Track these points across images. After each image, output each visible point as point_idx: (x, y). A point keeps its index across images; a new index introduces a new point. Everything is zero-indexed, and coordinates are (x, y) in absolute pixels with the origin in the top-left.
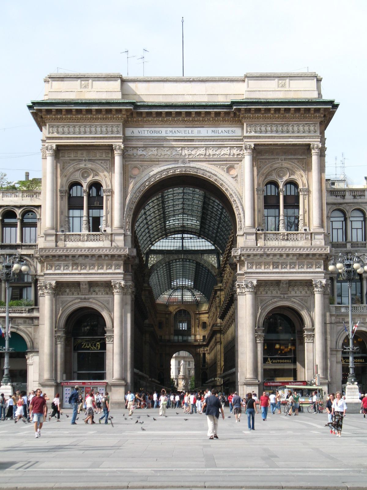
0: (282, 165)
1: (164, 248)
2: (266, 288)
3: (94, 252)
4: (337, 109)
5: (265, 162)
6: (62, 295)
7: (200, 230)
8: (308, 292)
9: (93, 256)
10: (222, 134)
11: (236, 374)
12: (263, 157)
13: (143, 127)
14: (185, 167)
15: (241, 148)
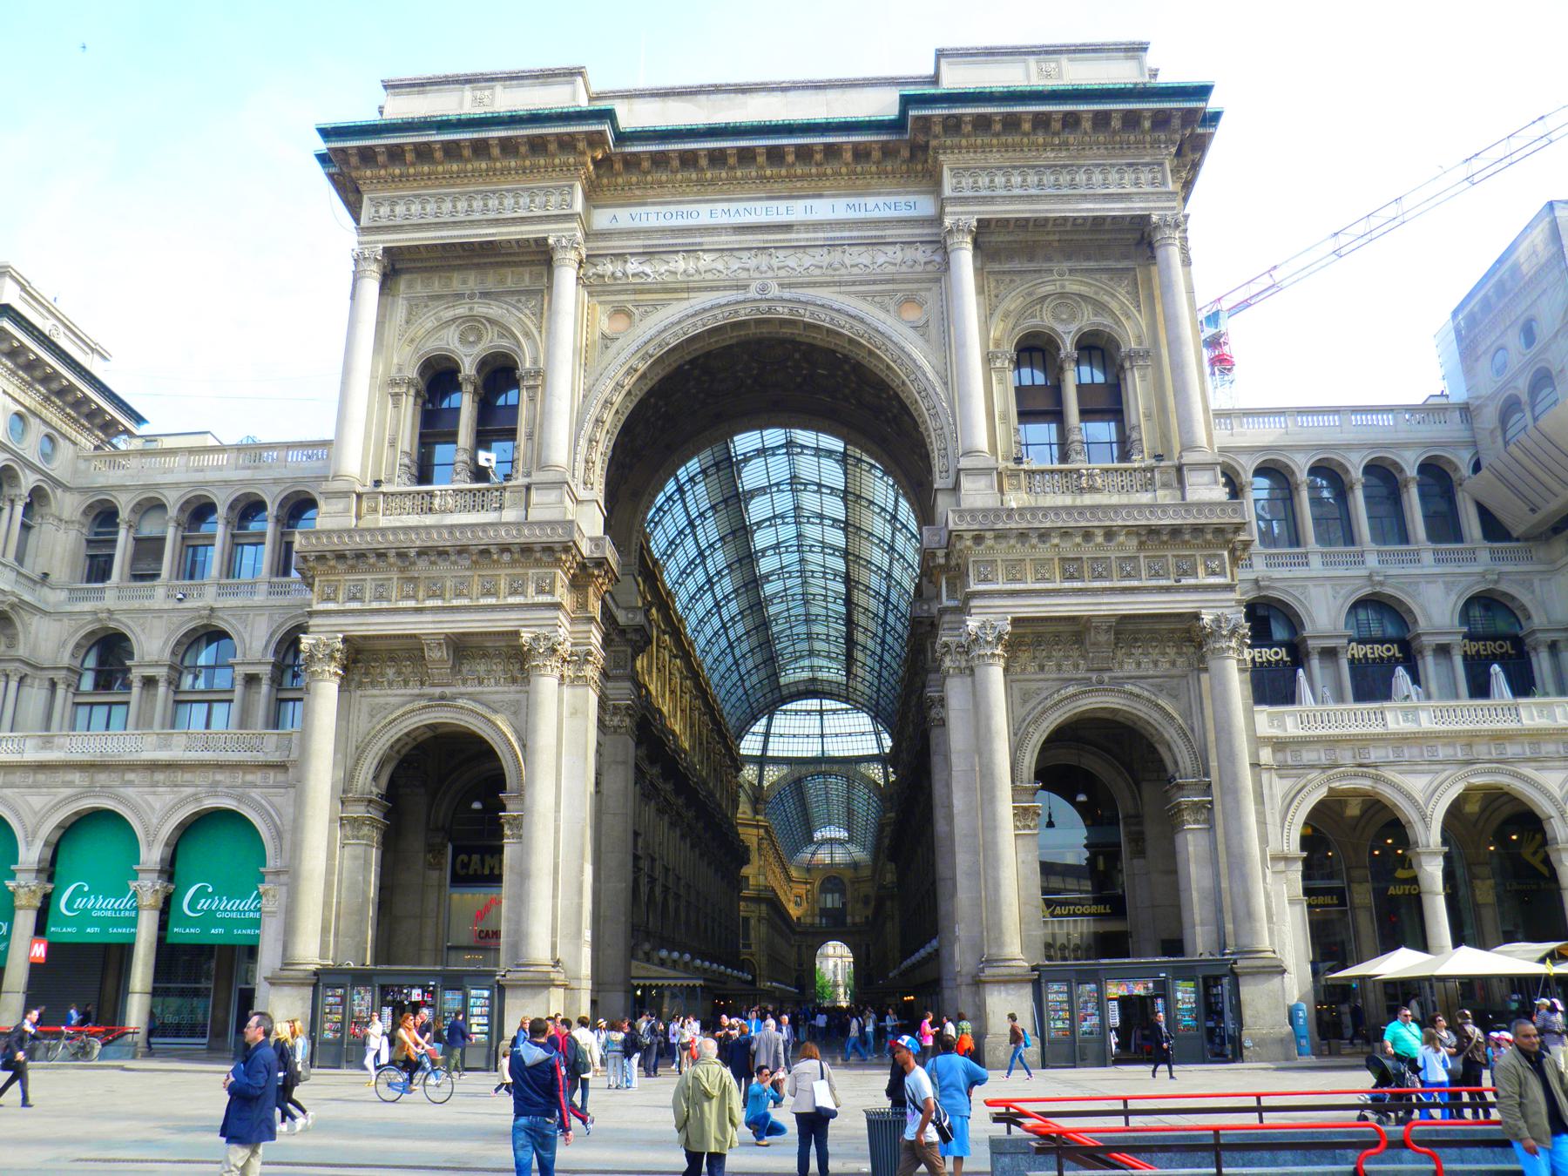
0: (1063, 287)
1: (790, 755)
2: (1037, 654)
3: (467, 538)
4: (1215, 126)
5: (1011, 281)
6: (373, 687)
7: (847, 685)
8: (1180, 661)
9: (462, 550)
10: (876, 214)
11: (944, 952)
12: (1007, 267)
13: (645, 204)
14: (767, 300)
15: (935, 246)
